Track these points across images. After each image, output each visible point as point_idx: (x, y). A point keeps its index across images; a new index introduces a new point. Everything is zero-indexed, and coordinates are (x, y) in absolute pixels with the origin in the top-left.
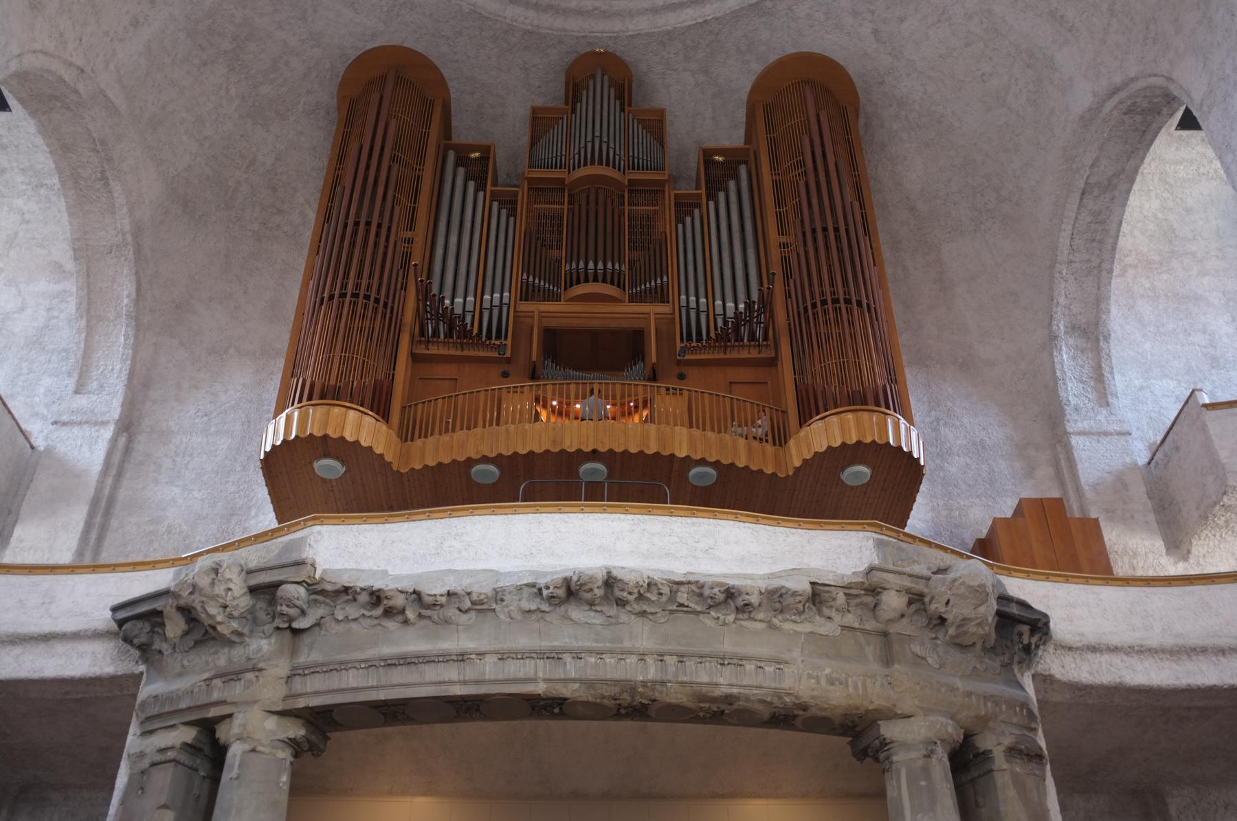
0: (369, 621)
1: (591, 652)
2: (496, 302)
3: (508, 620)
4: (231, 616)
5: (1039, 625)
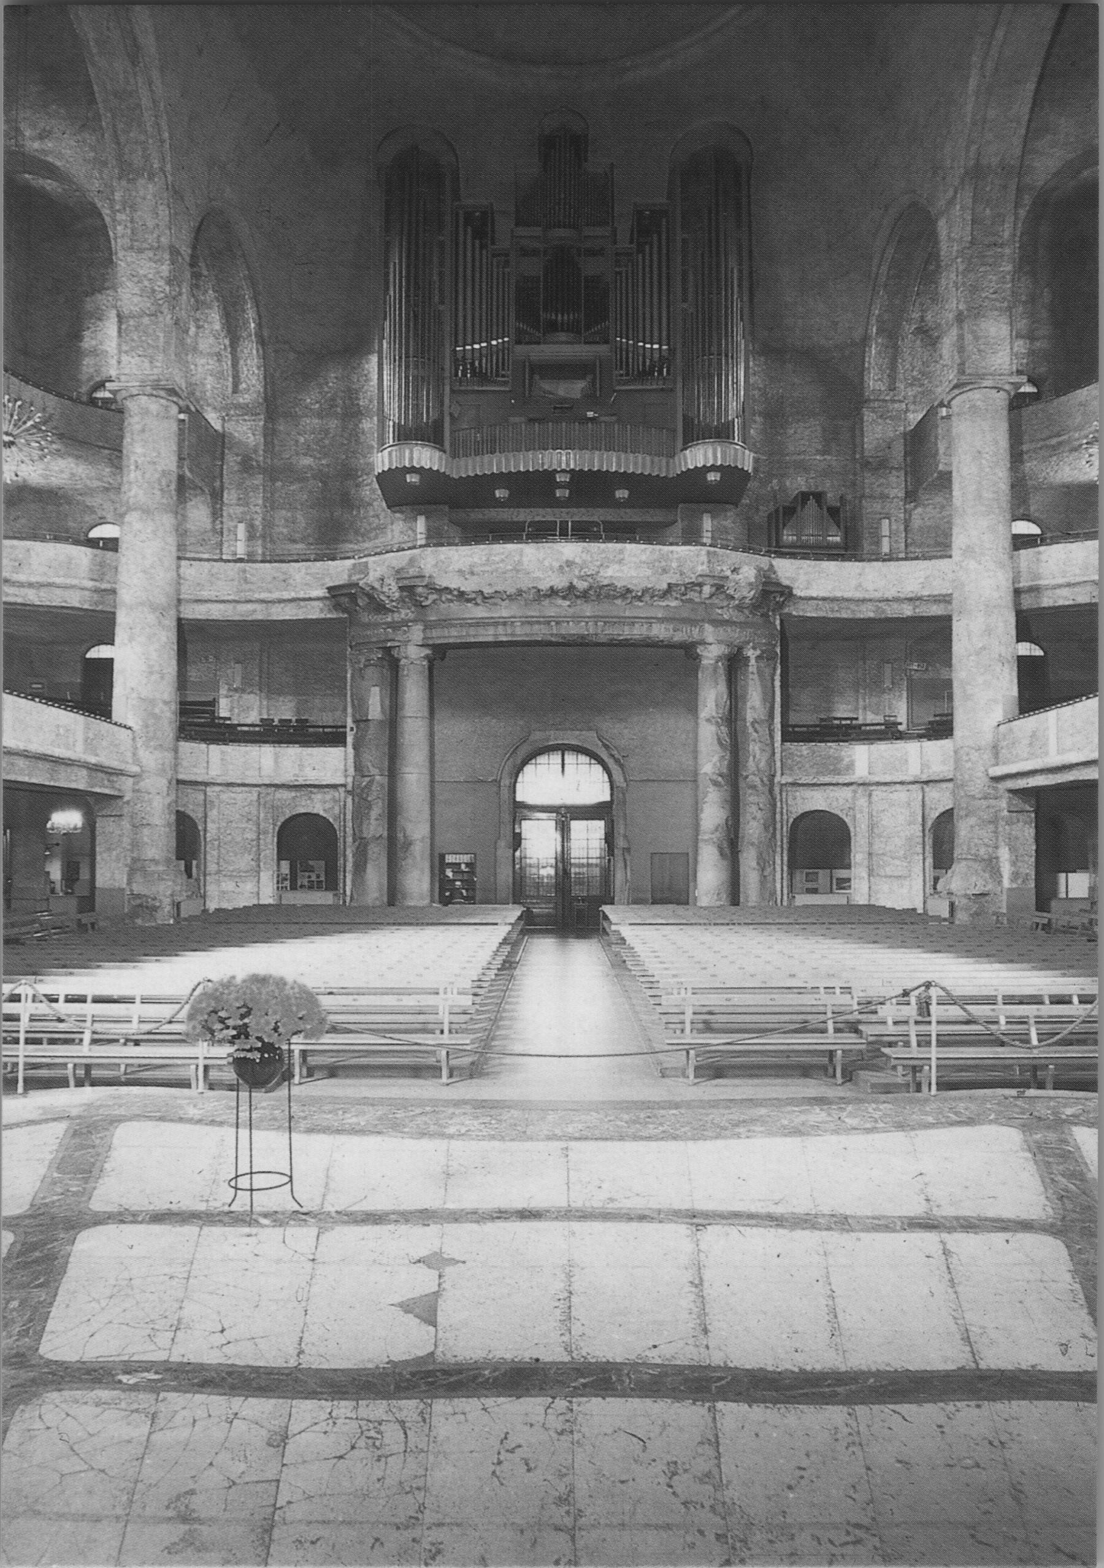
5: (787, 593)
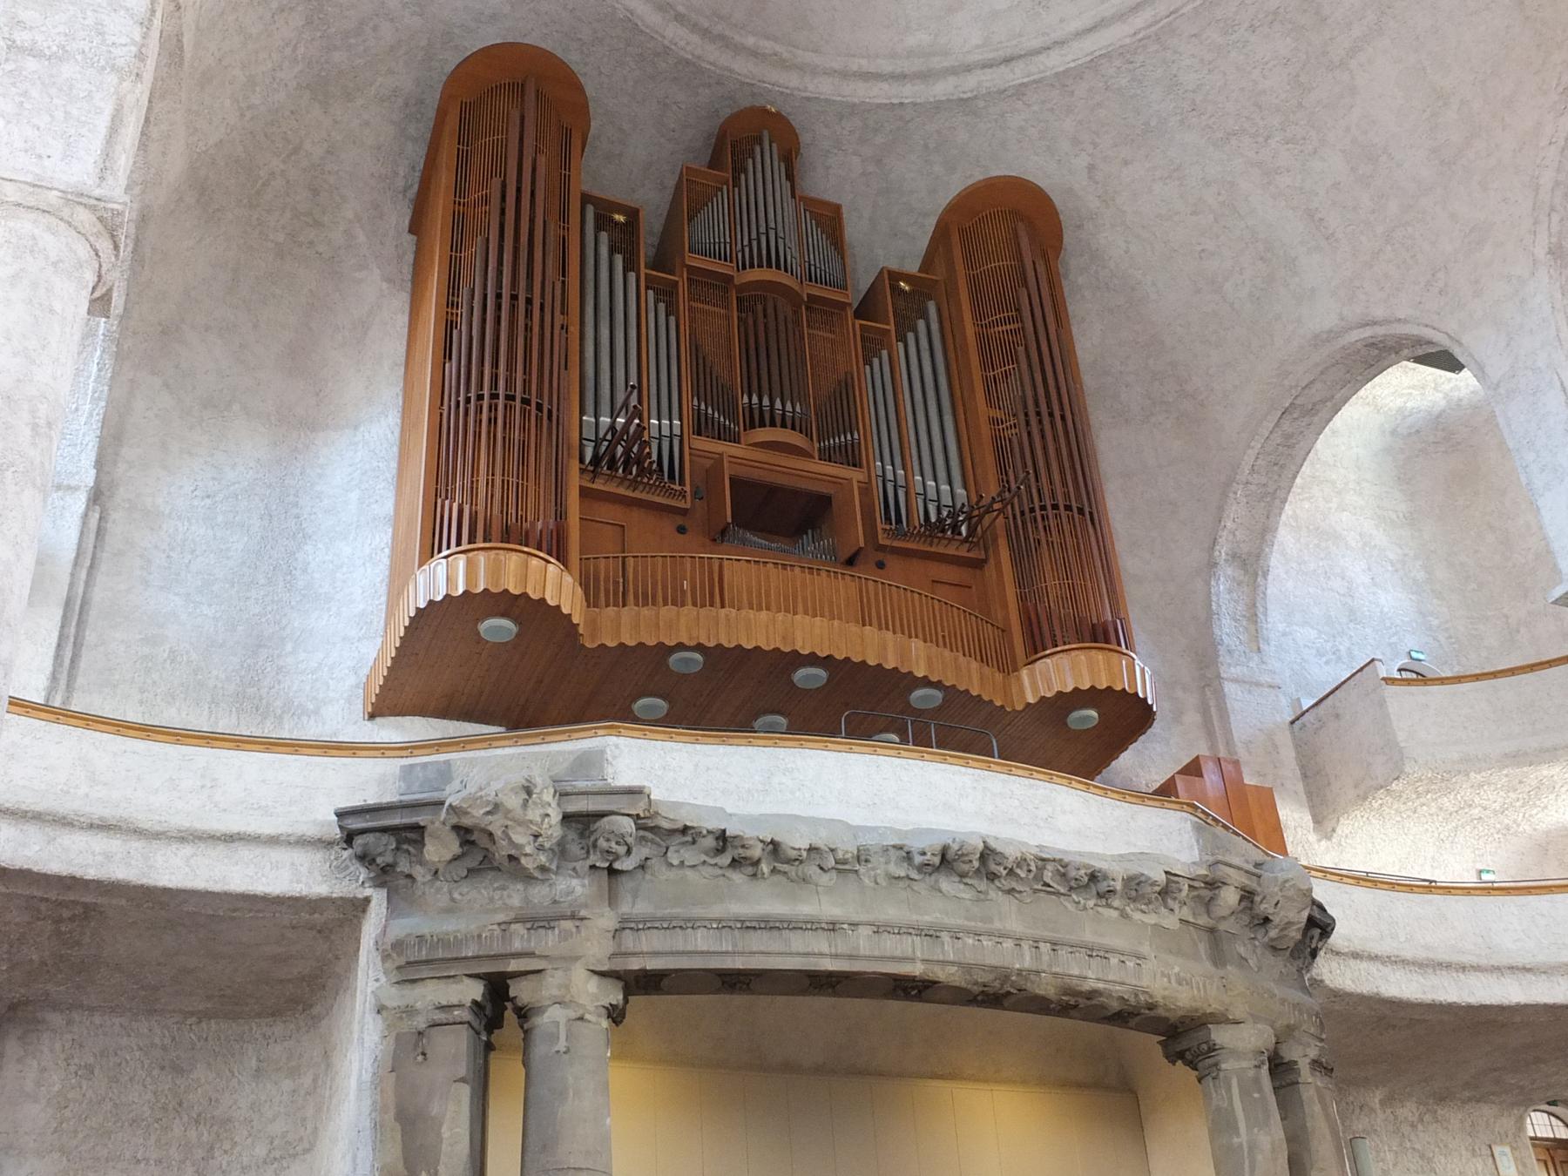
0: (710, 869)
1: (968, 932)
2: (665, 432)
3: (872, 884)
4: (541, 848)
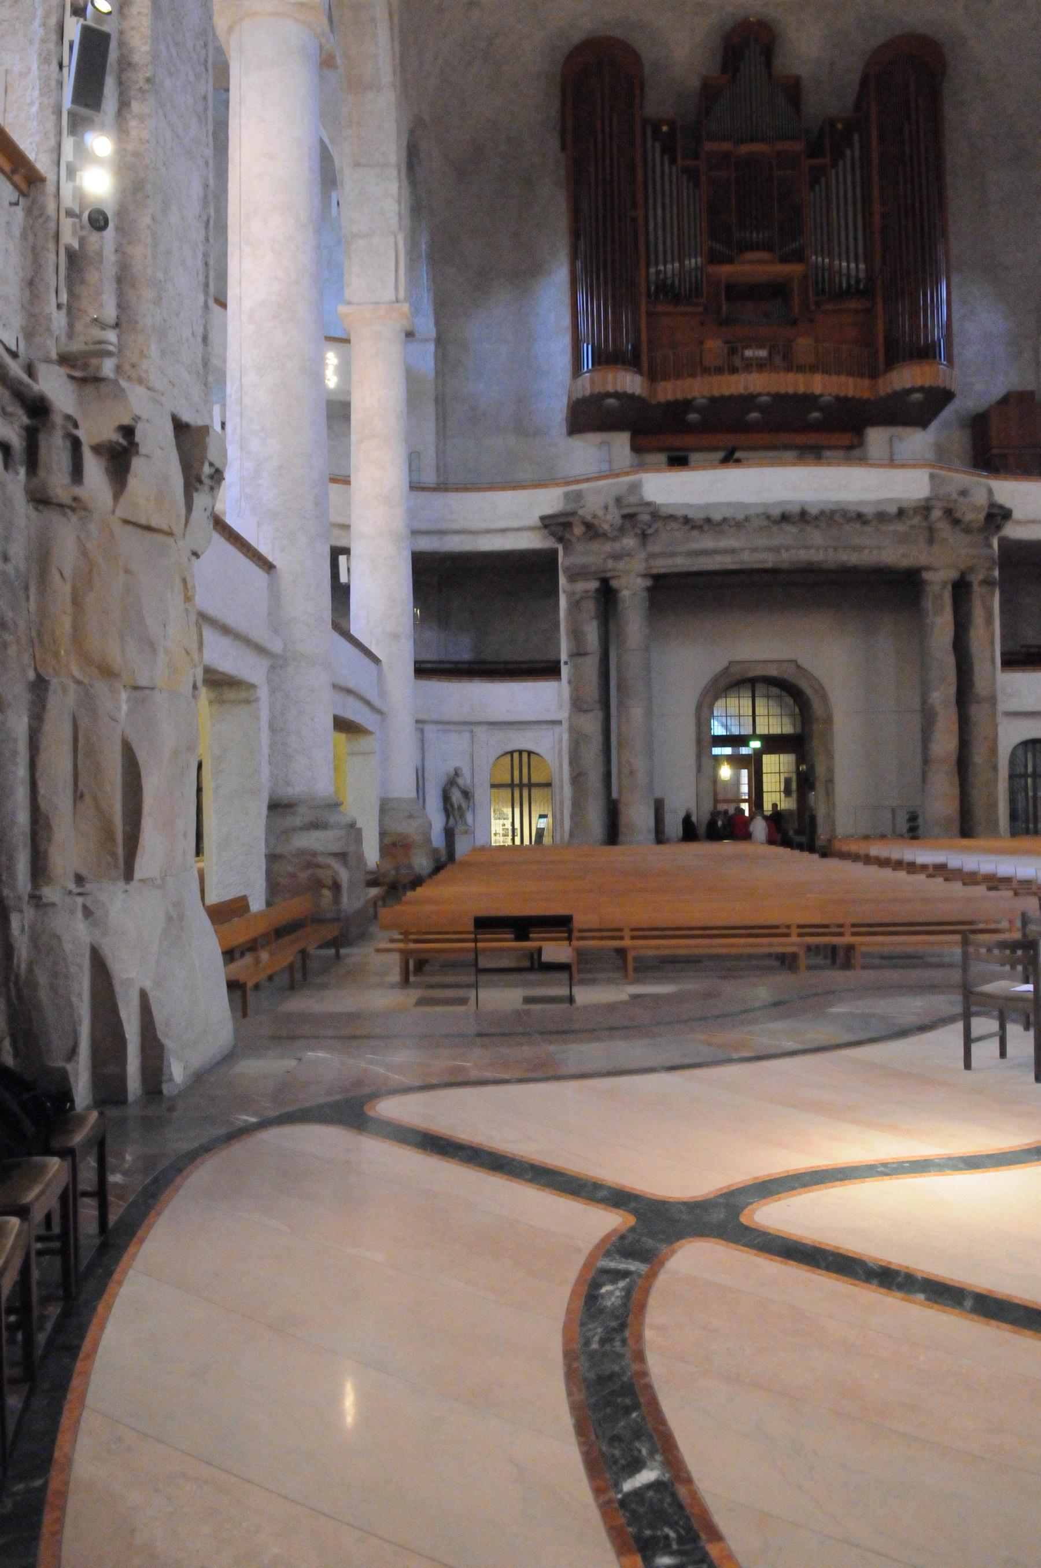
5: (1006, 514)
